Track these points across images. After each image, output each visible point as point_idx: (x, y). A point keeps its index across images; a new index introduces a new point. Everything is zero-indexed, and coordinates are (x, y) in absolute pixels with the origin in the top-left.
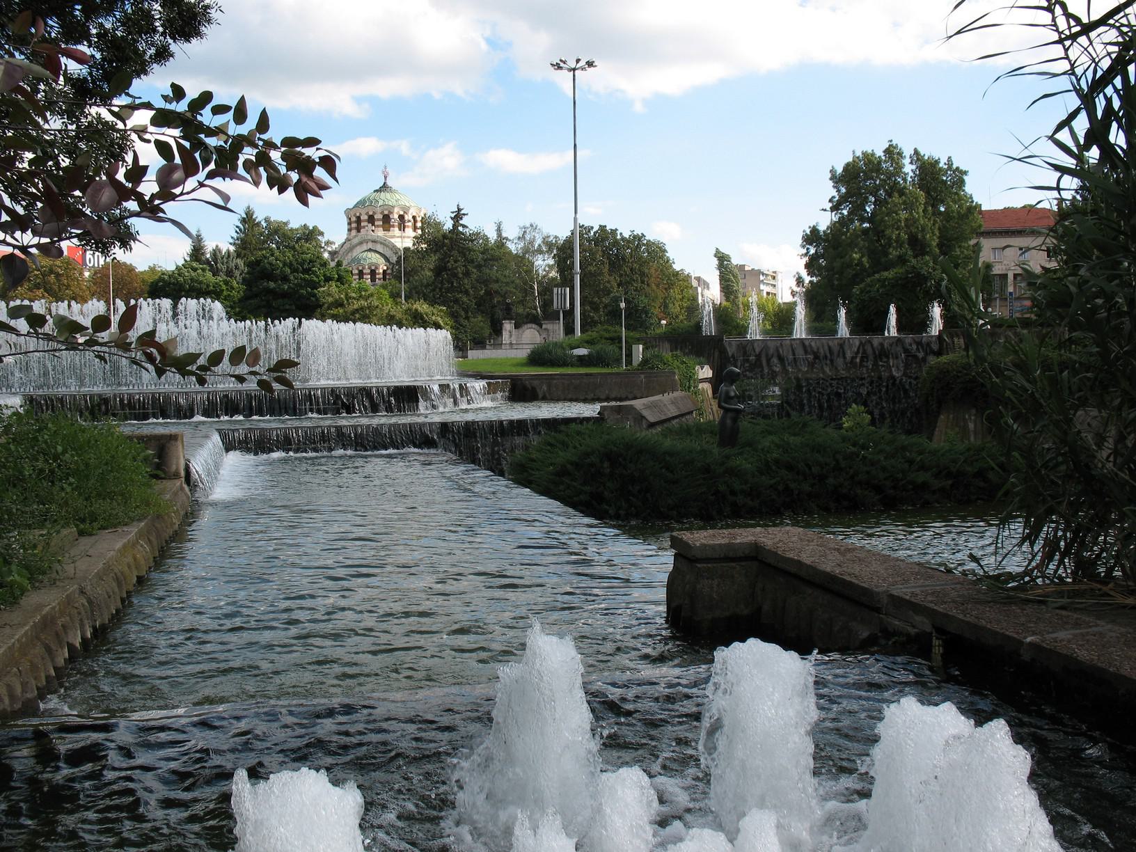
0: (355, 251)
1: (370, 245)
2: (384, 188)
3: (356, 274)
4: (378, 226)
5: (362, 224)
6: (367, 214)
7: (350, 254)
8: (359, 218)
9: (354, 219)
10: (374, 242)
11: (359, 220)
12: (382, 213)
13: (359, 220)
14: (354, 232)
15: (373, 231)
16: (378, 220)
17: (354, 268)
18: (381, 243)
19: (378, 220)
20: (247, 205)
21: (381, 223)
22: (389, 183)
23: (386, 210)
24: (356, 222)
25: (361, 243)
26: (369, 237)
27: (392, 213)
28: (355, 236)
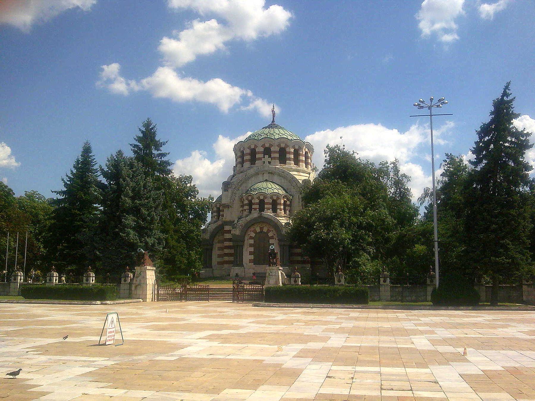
0: (250, 181)
4: (274, 158)
5: (258, 156)
7: (244, 185)
9: (239, 154)
11: (253, 153)
12: (279, 145)
13: (253, 153)
15: (269, 163)
16: (275, 152)
18: (279, 175)
19: (275, 152)
20: (145, 120)
21: (277, 155)
22: (276, 123)
24: (240, 157)
28: (249, 168)
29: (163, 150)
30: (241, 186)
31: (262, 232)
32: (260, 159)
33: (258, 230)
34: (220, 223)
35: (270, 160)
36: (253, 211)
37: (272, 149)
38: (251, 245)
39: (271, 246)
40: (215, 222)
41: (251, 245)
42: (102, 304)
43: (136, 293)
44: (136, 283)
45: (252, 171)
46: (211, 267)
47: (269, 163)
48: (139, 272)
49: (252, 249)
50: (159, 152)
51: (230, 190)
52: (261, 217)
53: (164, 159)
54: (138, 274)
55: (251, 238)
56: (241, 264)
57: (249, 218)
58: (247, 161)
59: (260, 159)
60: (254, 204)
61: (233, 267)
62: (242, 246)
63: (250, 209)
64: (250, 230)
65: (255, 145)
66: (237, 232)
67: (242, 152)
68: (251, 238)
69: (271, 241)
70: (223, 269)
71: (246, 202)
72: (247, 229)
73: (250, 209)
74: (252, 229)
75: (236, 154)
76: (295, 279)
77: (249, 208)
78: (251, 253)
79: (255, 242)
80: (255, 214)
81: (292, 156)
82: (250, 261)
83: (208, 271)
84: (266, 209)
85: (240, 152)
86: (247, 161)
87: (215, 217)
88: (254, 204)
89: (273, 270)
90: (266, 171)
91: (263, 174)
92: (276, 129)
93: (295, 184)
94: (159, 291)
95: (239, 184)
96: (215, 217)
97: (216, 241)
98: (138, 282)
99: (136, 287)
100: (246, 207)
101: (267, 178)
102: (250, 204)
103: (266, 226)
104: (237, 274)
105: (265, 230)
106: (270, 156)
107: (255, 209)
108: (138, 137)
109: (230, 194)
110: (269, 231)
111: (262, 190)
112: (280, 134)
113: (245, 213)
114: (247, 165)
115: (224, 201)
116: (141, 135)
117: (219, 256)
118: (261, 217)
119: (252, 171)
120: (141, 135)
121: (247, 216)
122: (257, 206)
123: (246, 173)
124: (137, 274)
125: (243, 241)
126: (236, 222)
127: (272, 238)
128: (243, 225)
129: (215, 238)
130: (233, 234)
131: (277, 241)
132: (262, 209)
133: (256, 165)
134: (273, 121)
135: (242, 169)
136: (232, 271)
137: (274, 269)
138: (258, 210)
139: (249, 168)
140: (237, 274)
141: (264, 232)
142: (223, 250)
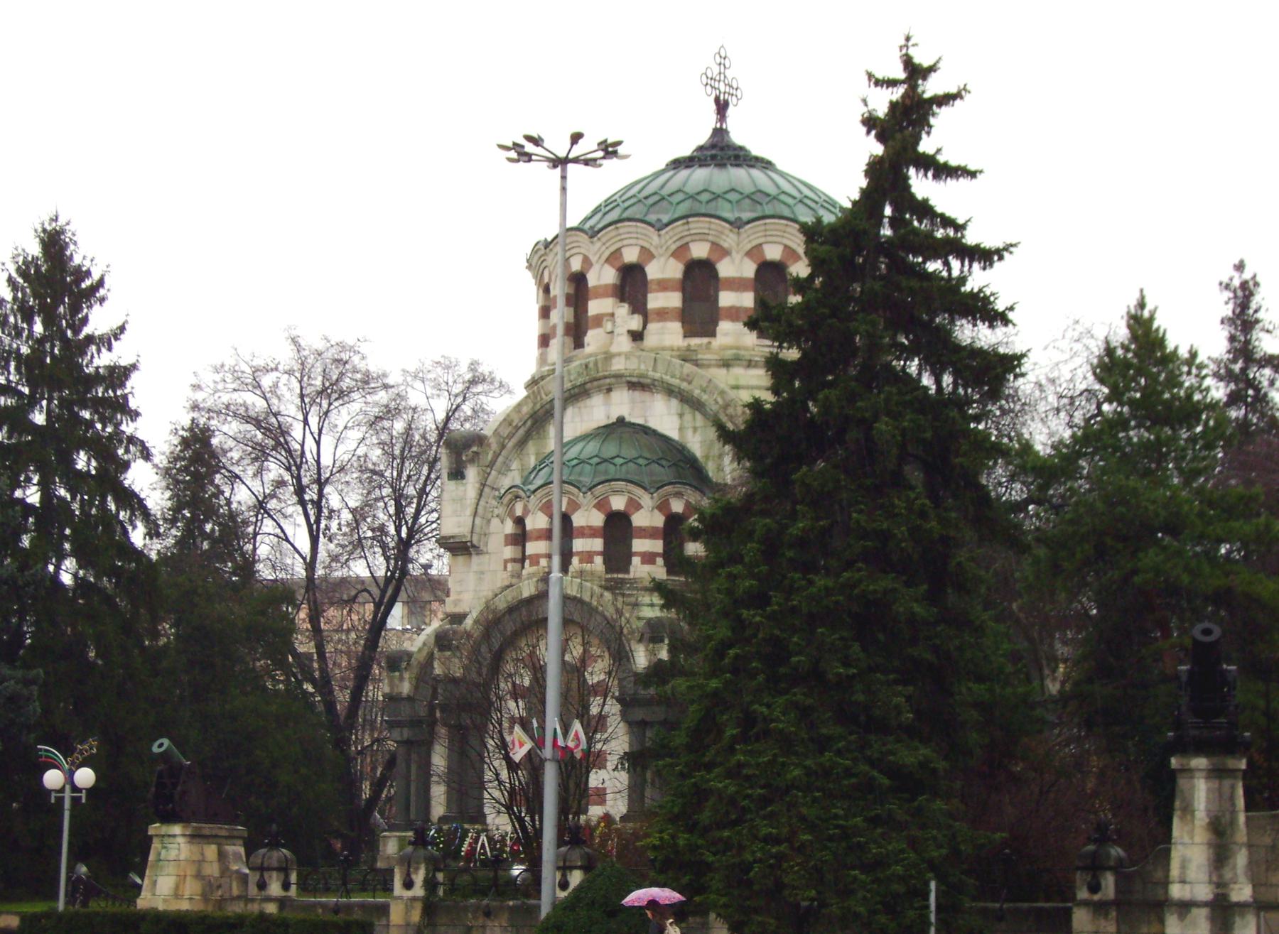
1: (621, 405)
6: (614, 257)
7: (531, 448)
15: (637, 336)
16: (664, 285)
23: (702, 237)
51: (472, 473)
76: (262, 876)
90: (618, 376)
91: (609, 390)
123: (539, 392)
134: (720, 133)
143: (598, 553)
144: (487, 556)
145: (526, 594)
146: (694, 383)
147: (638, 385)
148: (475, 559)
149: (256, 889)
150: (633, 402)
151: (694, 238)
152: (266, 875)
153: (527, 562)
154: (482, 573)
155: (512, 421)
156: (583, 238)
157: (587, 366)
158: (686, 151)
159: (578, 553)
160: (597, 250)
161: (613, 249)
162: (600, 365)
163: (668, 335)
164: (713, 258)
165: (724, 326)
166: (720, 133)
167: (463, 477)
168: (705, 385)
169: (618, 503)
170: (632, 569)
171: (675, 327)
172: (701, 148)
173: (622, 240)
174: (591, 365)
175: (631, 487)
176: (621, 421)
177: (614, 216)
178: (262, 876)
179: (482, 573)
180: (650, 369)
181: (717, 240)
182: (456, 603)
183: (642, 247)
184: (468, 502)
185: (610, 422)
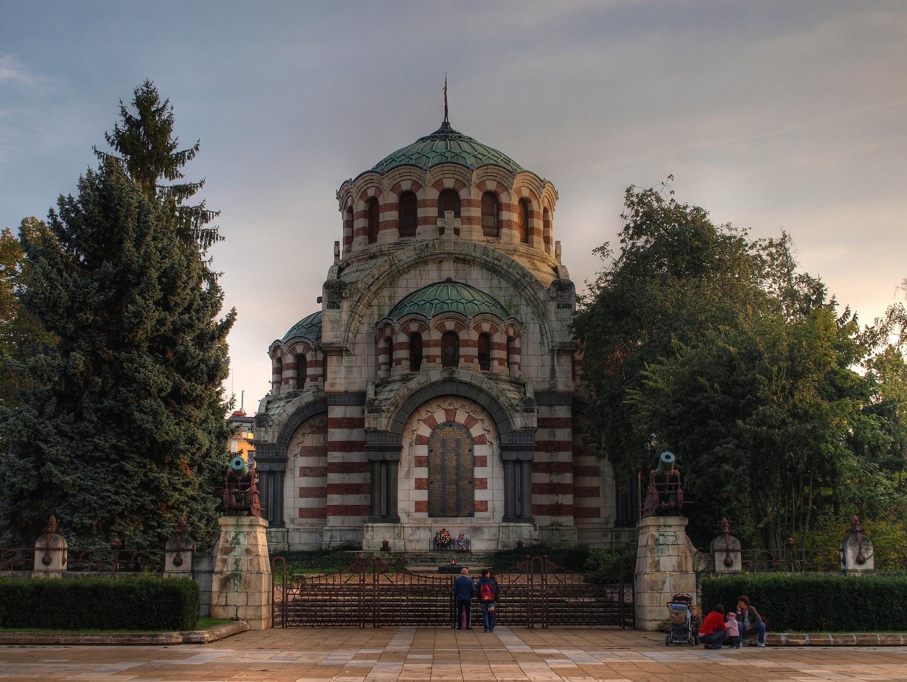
0: (402, 282)
2: (445, 132)
3: (401, 346)
4: (469, 220)
5: (421, 212)
6: (395, 188)
7: (386, 292)
8: (373, 203)
10: (463, 260)
14: (360, 241)
16: (470, 203)
17: (397, 327)
21: (476, 212)
25: (421, 262)
26: (450, 248)
27: (506, 189)
28: (398, 245)
29: (188, 173)
30: (376, 293)
31: (450, 423)
32: (426, 220)
33: (440, 417)
34: (307, 397)
35: (457, 223)
36: (424, 364)
37: (463, 194)
38: (420, 462)
39: (668, 453)
40: (291, 396)
41: (420, 462)
42: (187, 642)
43: (223, 603)
44: (225, 569)
45: (406, 255)
46: (282, 524)
47: (457, 231)
48: (233, 535)
49: (423, 473)
50: (177, 182)
51: (345, 305)
52: (451, 380)
53: (189, 202)
54: (230, 539)
55: (420, 440)
56: (390, 516)
57: (413, 385)
58: (388, 224)
59: (426, 220)
60: (429, 344)
61: (370, 525)
62: (397, 462)
63: (416, 362)
64: (417, 417)
65: (415, 183)
66: (383, 423)
67: (373, 203)
68: (420, 440)
69: (480, 450)
70: (327, 528)
71: (402, 338)
72: (412, 414)
73: (416, 362)
74: (424, 415)
75: (347, 209)
76: (728, 556)
77: (409, 357)
78: (419, 485)
79: (430, 451)
80: (434, 373)
81: (515, 217)
82: (419, 506)
83: (273, 535)
84: (462, 360)
85: (366, 202)
86: (388, 224)
87: (291, 382)
88: (429, 344)
89: (668, 529)
91: (441, 262)
92: (451, 142)
93: (533, 293)
94: (287, 595)
95: (373, 289)
96: (291, 382)
97: (295, 449)
98: (229, 568)
99: (226, 582)
100: (403, 354)
101: (452, 275)
102: (416, 343)
103: (463, 406)
104: (385, 544)
105: (461, 417)
106: (457, 215)
107: (431, 359)
108: (117, 131)
109: (345, 317)
110: (471, 421)
111: (448, 304)
112: (480, 156)
113: (400, 370)
114: (388, 236)
115: (329, 336)
116: (123, 127)
117: (305, 493)
118: (451, 380)
119: (406, 255)
120: (123, 127)
121: (405, 379)
122: (436, 351)
123: (393, 258)
124: (227, 541)
125: (399, 449)
126: (371, 395)
127: (481, 440)
128: (401, 403)
129: (295, 441)
130: (369, 428)
131: (497, 451)
132: (450, 360)
133: (418, 238)
134: (446, 124)
135: (374, 248)
136: (368, 535)
137: (670, 526)
138: (439, 360)
139: (396, 244)
140: (385, 544)
141: (459, 424)
142: (325, 475)
143: (475, 357)
144: (354, 357)
145: (433, 380)
146: (502, 261)
147: (463, 260)
148: (345, 359)
149: (723, 566)
150: (457, 270)
151: (490, 178)
152: (732, 555)
153: (394, 363)
154: (351, 367)
155: (374, 275)
156: (376, 177)
157: (427, 246)
158: (428, 133)
159: (464, 356)
160: (386, 183)
161: (437, 179)
162: (436, 246)
163: (476, 235)
164: (499, 191)
165: (504, 231)
166: (446, 124)
167: (339, 308)
168: (510, 263)
169: (486, 327)
170: (491, 368)
171: (477, 228)
172: (435, 133)
173: (367, 184)
174: (431, 245)
175: (494, 319)
176: (449, 281)
177: (394, 164)
178: (728, 556)
179: (351, 367)
180: (472, 251)
181: (500, 181)
182: (333, 385)
183: (456, 179)
184: (343, 323)
185: (442, 281)
